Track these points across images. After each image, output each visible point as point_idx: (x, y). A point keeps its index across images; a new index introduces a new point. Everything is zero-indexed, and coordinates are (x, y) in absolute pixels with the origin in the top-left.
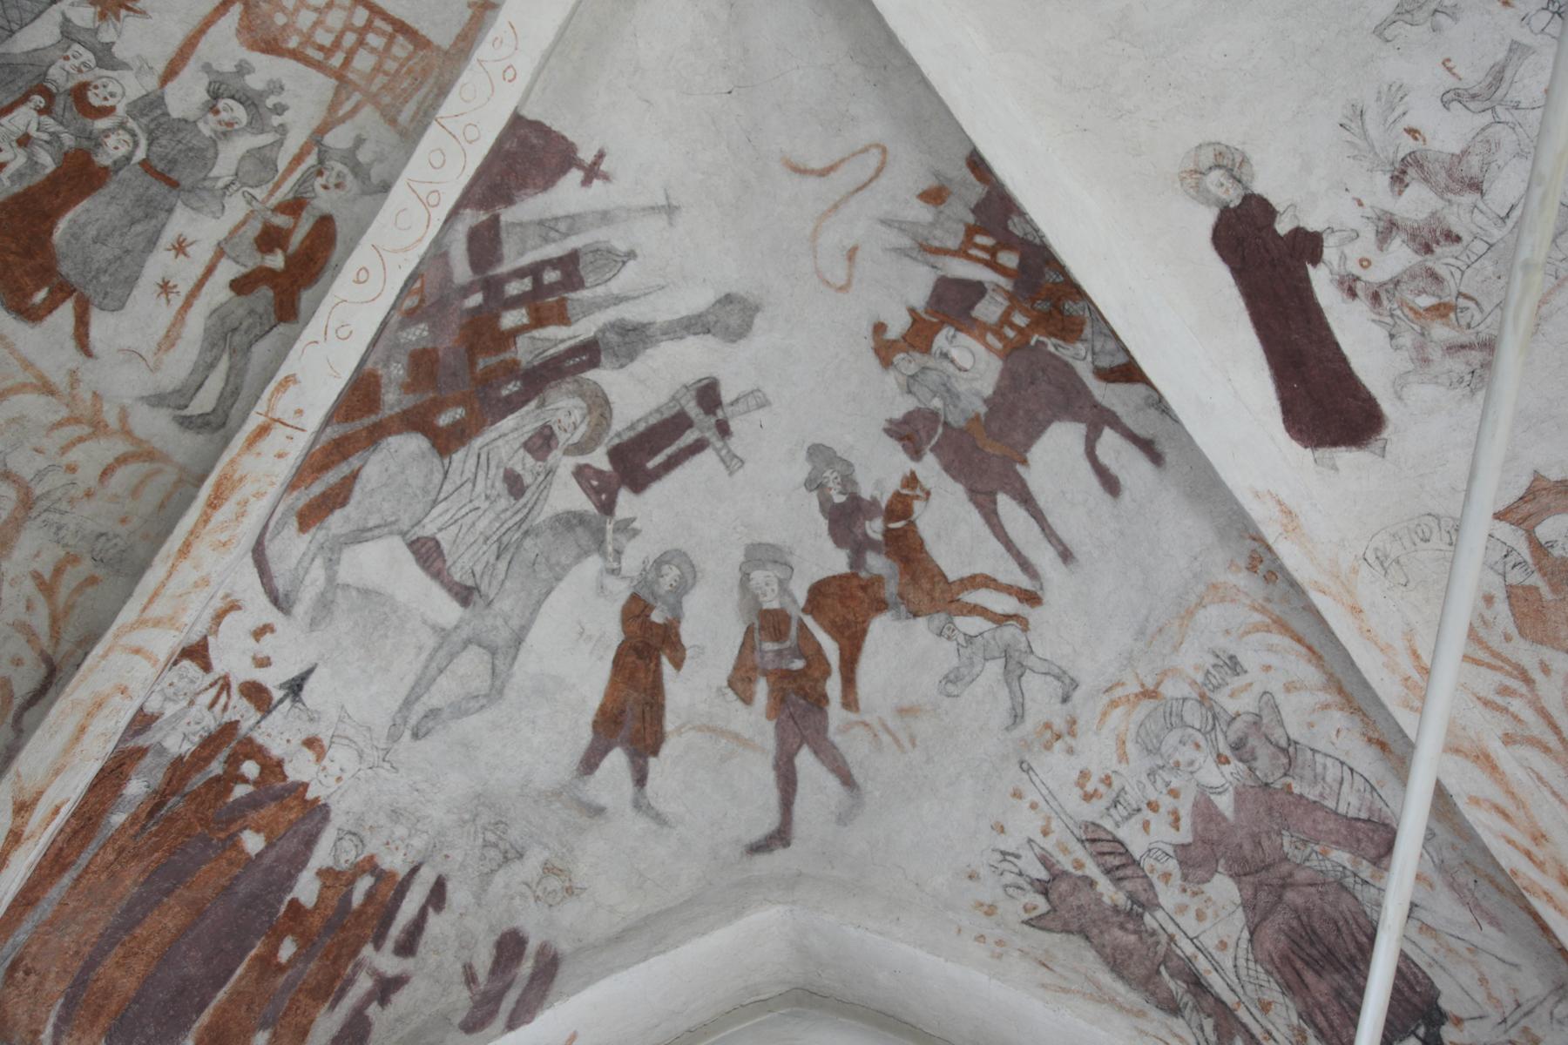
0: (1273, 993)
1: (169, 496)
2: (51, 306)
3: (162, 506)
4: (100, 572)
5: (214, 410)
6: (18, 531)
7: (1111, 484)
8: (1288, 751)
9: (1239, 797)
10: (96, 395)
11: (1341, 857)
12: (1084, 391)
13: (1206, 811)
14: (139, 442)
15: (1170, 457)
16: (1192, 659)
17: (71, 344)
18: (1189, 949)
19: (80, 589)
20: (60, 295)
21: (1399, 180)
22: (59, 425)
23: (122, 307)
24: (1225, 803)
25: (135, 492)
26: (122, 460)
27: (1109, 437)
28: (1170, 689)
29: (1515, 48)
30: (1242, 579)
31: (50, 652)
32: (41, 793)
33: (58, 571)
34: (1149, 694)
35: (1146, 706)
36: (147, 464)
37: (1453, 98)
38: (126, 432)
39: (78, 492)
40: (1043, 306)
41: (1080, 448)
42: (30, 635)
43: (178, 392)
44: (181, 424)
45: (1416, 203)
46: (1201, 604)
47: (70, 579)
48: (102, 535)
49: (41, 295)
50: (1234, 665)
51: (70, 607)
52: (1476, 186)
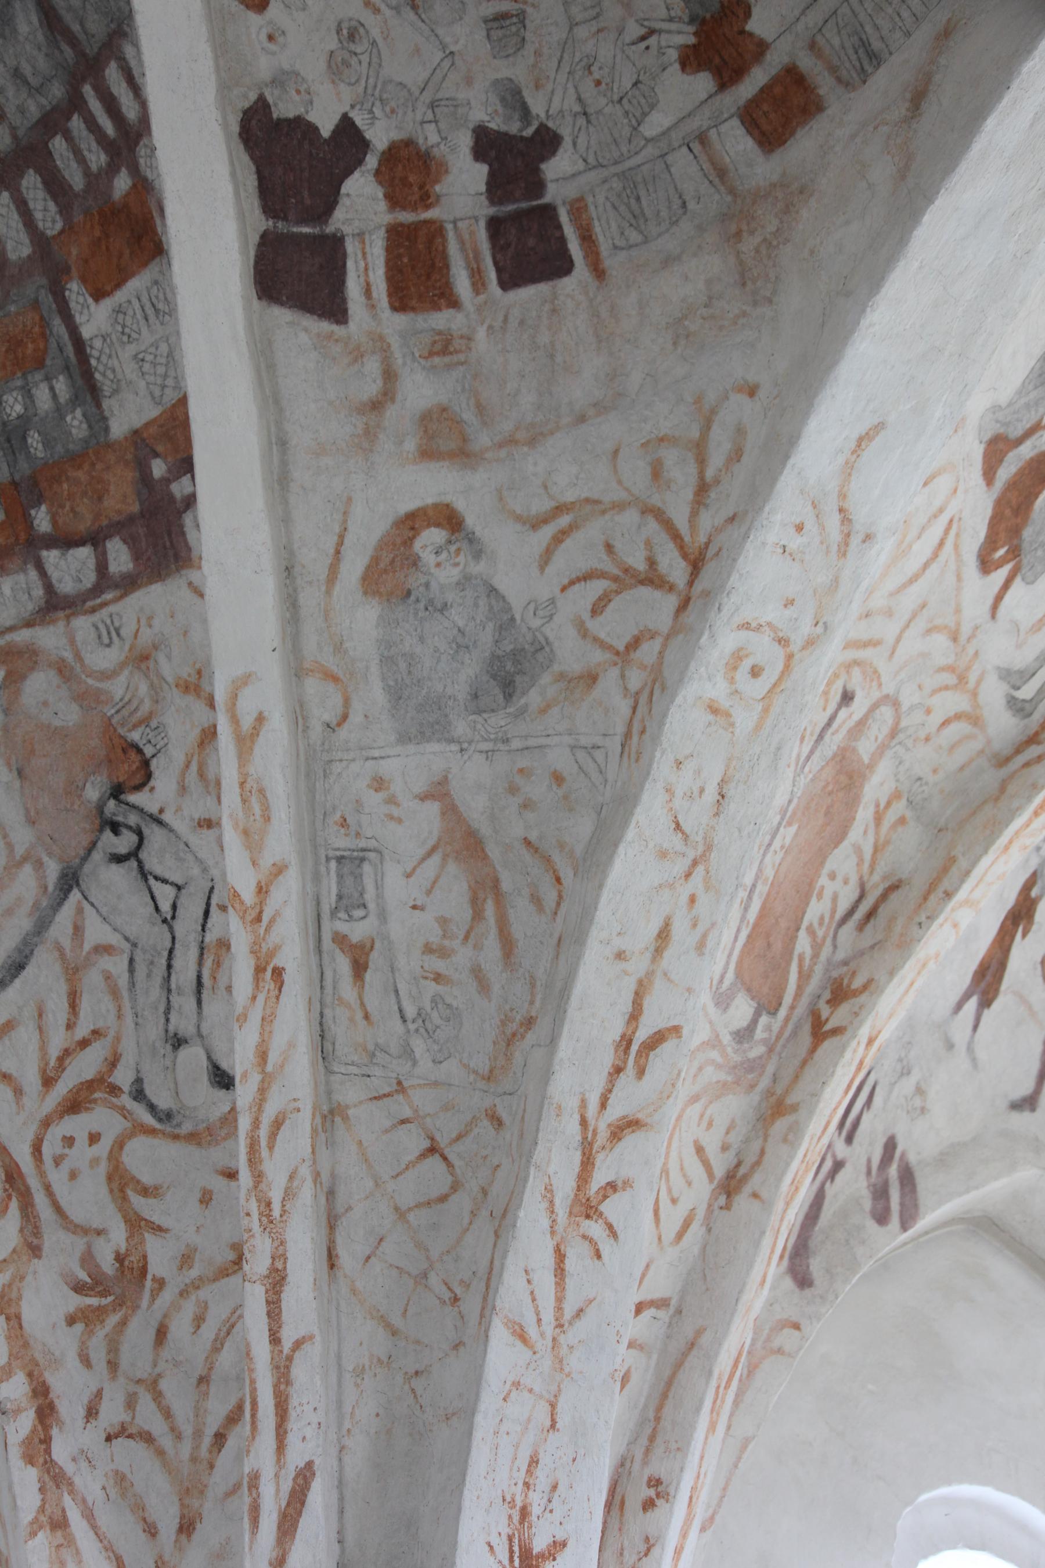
1: (971, 761)
2: (999, 565)
3: (962, 768)
4: (909, 814)
5: (1031, 700)
6: (881, 758)
10: (976, 654)
14: (976, 705)
17: (990, 601)
19: (894, 827)
20: (1011, 556)
22: (942, 669)
23: (1033, 582)
25: (952, 748)
26: (958, 717)
31: (865, 878)
32: (880, 1032)
33: (889, 804)
36: (970, 727)
38: (975, 694)
39: (922, 735)
42: (861, 861)
43: (1021, 672)
44: (1009, 702)
47: (890, 817)
48: (920, 779)
49: (1001, 552)
51: (887, 842)
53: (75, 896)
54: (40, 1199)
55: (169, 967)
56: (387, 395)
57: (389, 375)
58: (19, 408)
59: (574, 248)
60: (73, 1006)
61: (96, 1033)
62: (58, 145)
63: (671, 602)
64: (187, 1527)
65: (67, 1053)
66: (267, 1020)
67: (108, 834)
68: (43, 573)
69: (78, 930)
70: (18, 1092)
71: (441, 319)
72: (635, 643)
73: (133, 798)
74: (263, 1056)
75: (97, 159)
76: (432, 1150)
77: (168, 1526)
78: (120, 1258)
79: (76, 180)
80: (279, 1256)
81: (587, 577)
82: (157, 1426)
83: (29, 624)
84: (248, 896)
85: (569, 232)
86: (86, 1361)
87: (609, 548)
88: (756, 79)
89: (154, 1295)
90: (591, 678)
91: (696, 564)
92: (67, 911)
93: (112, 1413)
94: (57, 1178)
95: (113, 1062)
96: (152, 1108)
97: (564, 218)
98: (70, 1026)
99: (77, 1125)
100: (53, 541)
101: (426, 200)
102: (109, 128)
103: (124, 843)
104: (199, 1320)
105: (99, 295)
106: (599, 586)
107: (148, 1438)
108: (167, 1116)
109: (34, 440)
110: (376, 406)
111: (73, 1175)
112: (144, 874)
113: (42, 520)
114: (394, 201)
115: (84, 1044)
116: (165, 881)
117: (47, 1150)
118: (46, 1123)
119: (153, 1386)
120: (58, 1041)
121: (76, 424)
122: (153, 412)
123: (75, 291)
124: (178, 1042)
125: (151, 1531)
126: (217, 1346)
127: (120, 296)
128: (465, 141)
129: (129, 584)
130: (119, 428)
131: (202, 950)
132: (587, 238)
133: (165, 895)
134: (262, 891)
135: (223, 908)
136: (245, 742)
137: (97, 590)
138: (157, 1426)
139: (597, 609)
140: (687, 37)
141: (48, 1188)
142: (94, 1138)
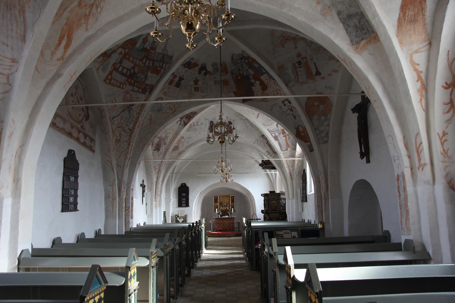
0: (155, 145)
7: (177, 123)
8: (167, 138)
9: (163, 138)
11: (163, 143)
12: (182, 120)
13: (162, 137)
15: (180, 126)
16: (169, 131)
18: (154, 140)
21: (197, 123)
24: (162, 137)
27: (180, 122)
28: (167, 131)
29: (204, 124)
30: (175, 132)
34: (166, 130)
35: (165, 131)
37: (201, 123)
40: (187, 116)
41: (178, 120)
45: (196, 124)
46: (173, 130)
50: (170, 134)
52: (197, 126)
53: (124, 112)
54: (114, 133)
55: (129, 120)
56: (164, 89)
57: (165, 88)
58: (139, 76)
59: (180, 87)
60: (121, 120)
61: (122, 123)
62: (156, 62)
63: (172, 112)
64: (120, 157)
65: (119, 124)
66: (137, 129)
67: (128, 109)
68: (134, 88)
69: (123, 115)
70: (115, 125)
71: (170, 86)
72: (168, 113)
73: (132, 107)
74: (136, 131)
75: (158, 65)
76: (140, 138)
77: (119, 157)
78: (119, 139)
79: (155, 65)
80: (133, 144)
81: (168, 107)
82: (119, 150)
83: (130, 90)
84: (140, 121)
85: (181, 86)
86: (115, 145)
87: (170, 106)
88: (196, 86)
89: (121, 142)
90: (164, 113)
91: (175, 111)
92: (122, 113)
93: (116, 149)
94: (116, 132)
95: (122, 125)
96: (124, 130)
97: (181, 84)
98: (120, 122)
99: (118, 129)
100: (135, 86)
101: (174, 79)
102: (161, 65)
103: (129, 110)
104: (123, 145)
105: (151, 73)
106: (168, 108)
107: (118, 151)
108: (125, 130)
109: (139, 79)
110: (163, 90)
111: (117, 132)
112: (130, 113)
113: (136, 84)
114: (173, 78)
115: (121, 123)
116: (131, 114)
117: (116, 130)
118: (116, 128)
119: (119, 148)
120: (119, 122)
121: (143, 80)
122: (150, 84)
123: (149, 71)
124: (127, 125)
125: (118, 157)
126: (123, 147)
127: (153, 74)
128: (179, 76)
129: (140, 93)
130: (146, 82)
131: (132, 120)
132: (181, 87)
133: (130, 115)
134: (141, 121)
135: (134, 118)
136: (145, 111)
137: (137, 91)
138: (119, 150)
139: (167, 109)
140: (195, 80)
141: (115, 133)
142: (119, 130)
